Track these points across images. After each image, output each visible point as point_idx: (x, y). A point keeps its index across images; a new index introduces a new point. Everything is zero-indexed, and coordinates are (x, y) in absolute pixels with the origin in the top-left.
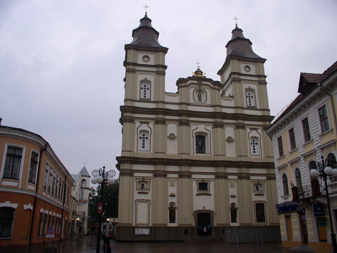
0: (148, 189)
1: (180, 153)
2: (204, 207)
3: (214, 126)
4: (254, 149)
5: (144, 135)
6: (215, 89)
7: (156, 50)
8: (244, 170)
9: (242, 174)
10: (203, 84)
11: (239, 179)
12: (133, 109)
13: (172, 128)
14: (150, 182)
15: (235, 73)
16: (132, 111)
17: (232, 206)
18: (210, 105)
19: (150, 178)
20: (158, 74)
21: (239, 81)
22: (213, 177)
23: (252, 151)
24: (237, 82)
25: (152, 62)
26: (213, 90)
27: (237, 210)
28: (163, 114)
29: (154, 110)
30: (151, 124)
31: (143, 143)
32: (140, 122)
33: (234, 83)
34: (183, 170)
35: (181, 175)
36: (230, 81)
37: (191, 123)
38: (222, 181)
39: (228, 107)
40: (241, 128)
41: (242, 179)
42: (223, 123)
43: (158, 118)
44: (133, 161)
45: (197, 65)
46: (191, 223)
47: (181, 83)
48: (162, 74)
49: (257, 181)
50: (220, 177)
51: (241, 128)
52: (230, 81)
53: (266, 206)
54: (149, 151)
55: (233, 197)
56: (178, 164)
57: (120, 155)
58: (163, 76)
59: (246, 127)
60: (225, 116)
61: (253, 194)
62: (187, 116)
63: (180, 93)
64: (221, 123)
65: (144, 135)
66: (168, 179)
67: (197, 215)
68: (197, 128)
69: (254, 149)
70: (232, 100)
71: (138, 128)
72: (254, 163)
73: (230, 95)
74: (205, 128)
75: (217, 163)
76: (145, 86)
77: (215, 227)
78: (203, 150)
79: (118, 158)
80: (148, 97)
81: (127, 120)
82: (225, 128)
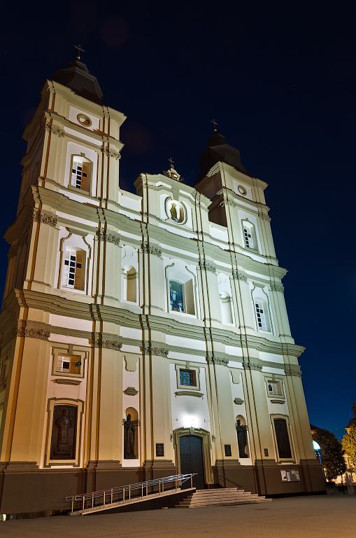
4: (259, 320)
53: (289, 424)
61: (269, 400)
69: (259, 320)
71: (62, 240)
77: (215, 469)
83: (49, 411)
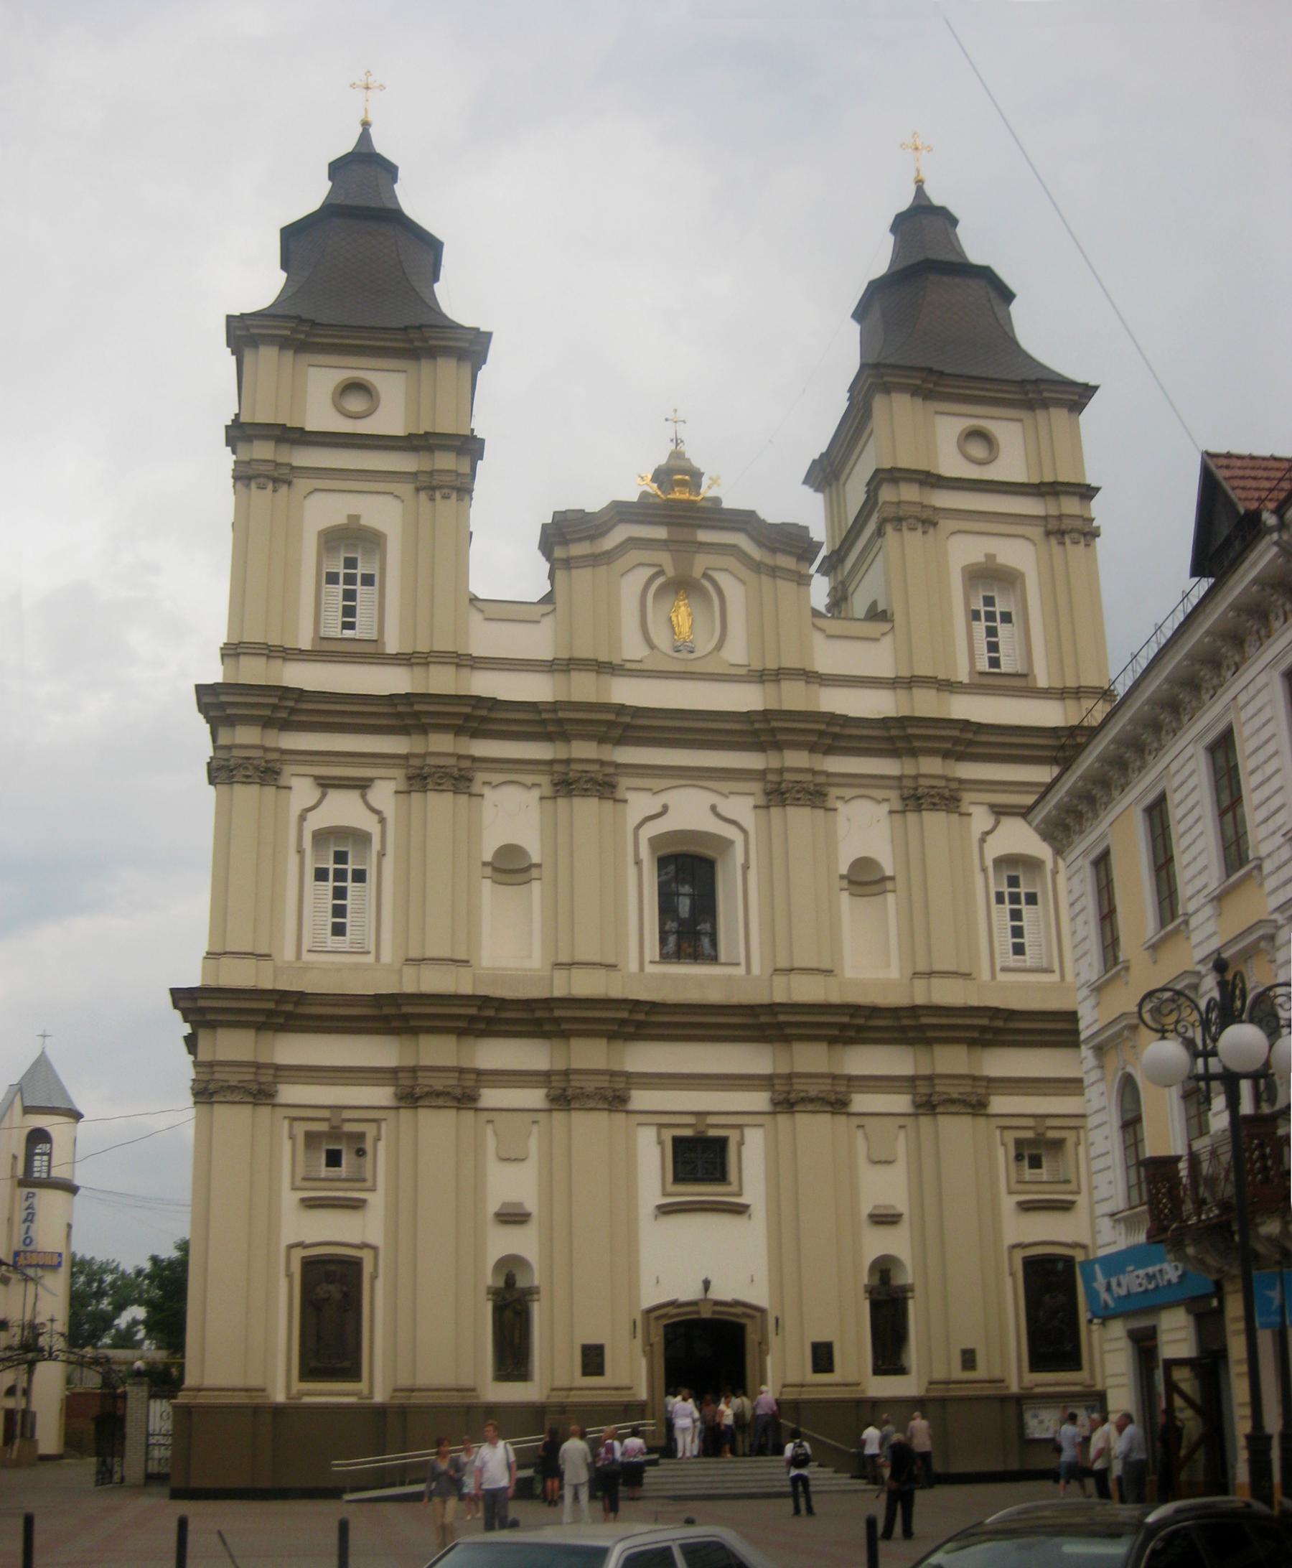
0: (364, 1180)
1: (559, 961)
2: (707, 1284)
3: (767, 794)
4: (1018, 932)
5: (341, 860)
6: (774, 572)
7: (417, 344)
8: (951, 1060)
9: (937, 1081)
10: (701, 544)
11: (921, 1111)
12: (275, 701)
13: (512, 813)
14: (378, 1139)
15: (897, 475)
16: (267, 712)
17: (877, 1277)
18: (743, 671)
19: (373, 1114)
20: (424, 488)
21: (928, 520)
22: (758, 1100)
23: (1005, 941)
24: (915, 529)
25: (390, 419)
26: (765, 580)
27: (911, 1304)
28: (458, 731)
29: (400, 709)
30: (384, 794)
31: (334, 906)
32: (316, 778)
34: (576, 1064)
35: (565, 1094)
36: (871, 526)
37: (624, 782)
38: (814, 1127)
39: (855, 674)
40: (934, 807)
41: (940, 1109)
42: (821, 779)
43: (424, 756)
44: (270, 1013)
46: (624, 1381)
47: (565, 542)
48: (453, 488)
49: (1031, 1122)
50: (803, 1100)
51: (934, 804)
52: (871, 526)
54: (372, 948)
55: (885, 1219)
56: (547, 1028)
57: (193, 979)
58: (460, 499)
59: (967, 797)
61: (1008, 1203)
62: (602, 740)
63: (560, 598)
64: (808, 777)
65: (341, 857)
66: (486, 1116)
67: (661, 1331)
68: (665, 809)
69: (1018, 932)
70: (883, 634)
71: (302, 818)
72: (1012, 1014)
73: (874, 604)
74: (713, 808)
75: (782, 1018)
76: (350, 563)
78: (706, 941)
79: (181, 998)
80: (364, 627)
81: (237, 767)
82: (839, 805)
83: (289, 1276)
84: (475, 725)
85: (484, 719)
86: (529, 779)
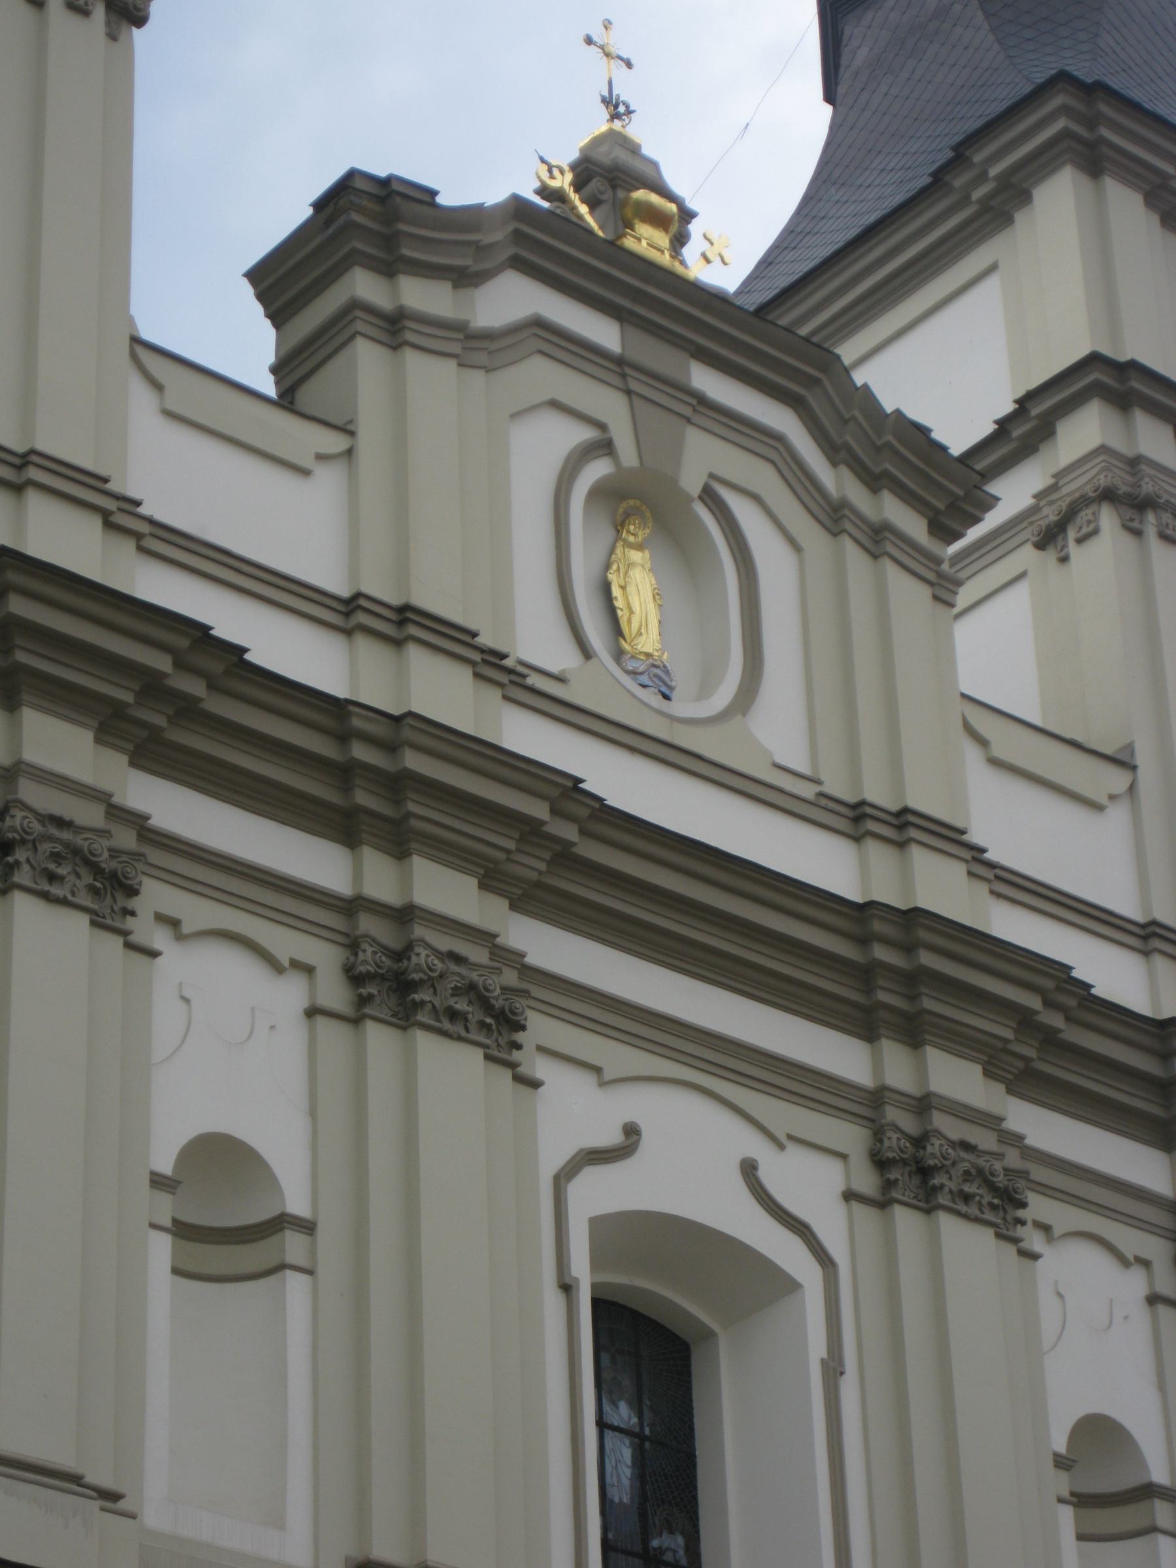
6: (878, 539)
10: (702, 402)
26: (855, 557)
33: (1127, 540)
45: (595, 73)
47: (389, 267)
60: (1050, 1040)
62: (492, 879)
74: (749, 1169)
84: (159, 720)
85: (188, 711)
86: (286, 942)
